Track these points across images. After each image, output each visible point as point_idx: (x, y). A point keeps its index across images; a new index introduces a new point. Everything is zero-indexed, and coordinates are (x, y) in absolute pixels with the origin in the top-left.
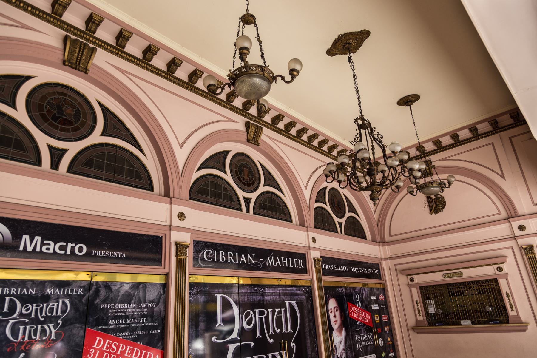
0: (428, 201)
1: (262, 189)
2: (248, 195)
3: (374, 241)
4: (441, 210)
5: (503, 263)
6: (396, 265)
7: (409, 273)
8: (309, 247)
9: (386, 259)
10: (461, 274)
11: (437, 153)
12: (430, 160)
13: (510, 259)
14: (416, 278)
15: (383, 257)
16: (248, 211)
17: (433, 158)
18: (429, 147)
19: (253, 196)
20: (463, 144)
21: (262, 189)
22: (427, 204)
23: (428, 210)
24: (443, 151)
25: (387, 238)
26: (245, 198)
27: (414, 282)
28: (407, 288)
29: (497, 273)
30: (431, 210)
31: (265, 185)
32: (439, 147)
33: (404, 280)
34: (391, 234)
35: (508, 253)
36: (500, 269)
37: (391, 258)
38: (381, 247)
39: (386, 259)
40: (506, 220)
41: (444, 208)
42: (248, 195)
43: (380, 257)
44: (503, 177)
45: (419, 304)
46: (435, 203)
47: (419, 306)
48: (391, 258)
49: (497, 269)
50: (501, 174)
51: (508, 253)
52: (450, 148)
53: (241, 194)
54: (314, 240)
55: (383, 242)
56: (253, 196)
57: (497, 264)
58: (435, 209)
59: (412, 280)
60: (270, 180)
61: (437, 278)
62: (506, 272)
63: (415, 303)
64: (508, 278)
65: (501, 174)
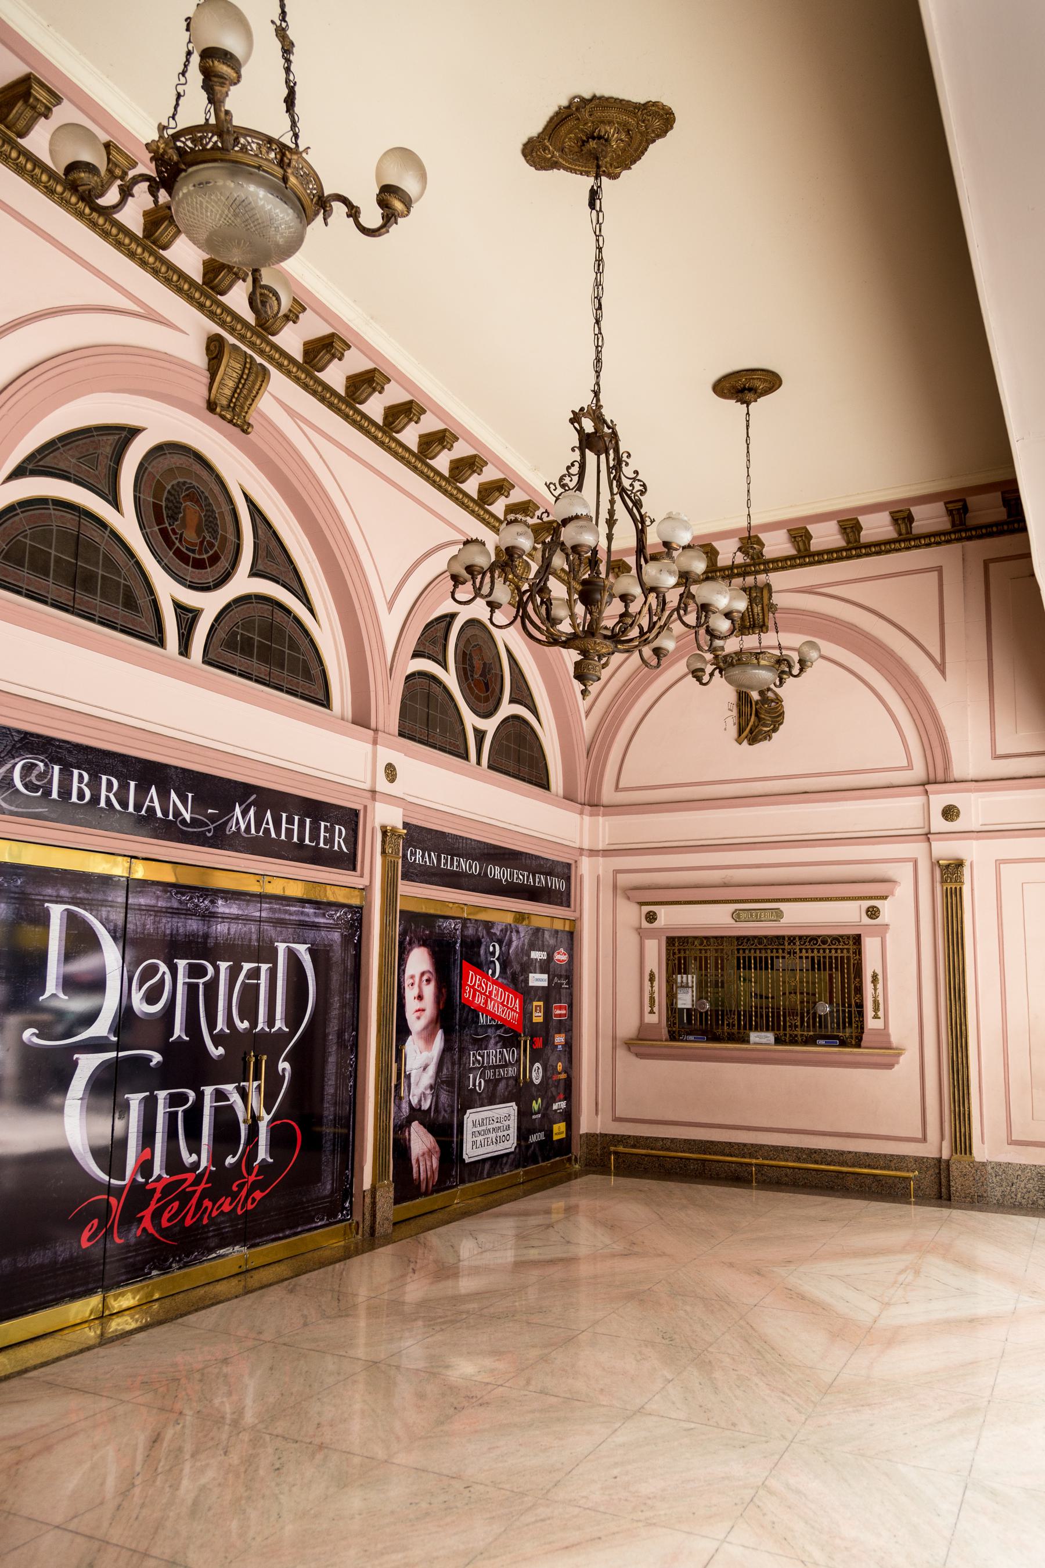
0: (739, 706)
1: (242, 583)
2: (191, 598)
3: (569, 797)
4: (768, 736)
5: (885, 898)
6: (617, 872)
7: (649, 898)
8: (373, 792)
9: (593, 853)
10: (779, 914)
11: (793, 567)
12: (768, 586)
13: (903, 891)
14: (662, 911)
15: (586, 846)
16: (185, 649)
17: (777, 580)
18: (777, 545)
19: (210, 604)
20: (867, 555)
21: (242, 583)
22: (735, 713)
23: (733, 730)
24: (811, 564)
25: (608, 794)
26: (179, 607)
27: (655, 925)
28: (634, 938)
29: (866, 920)
30: (740, 732)
31: (254, 573)
32: (804, 553)
33: (630, 914)
34: (621, 786)
35: (903, 874)
36: (873, 913)
37: (607, 853)
38: (587, 819)
39: (593, 853)
40: (921, 788)
41: (775, 730)
42: (191, 598)
43: (577, 845)
44: (942, 668)
45: (656, 984)
46: (757, 715)
47: (656, 989)
48: (607, 853)
49: (868, 911)
50: (938, 660)
51: (903, 874)
52: (830, 561)
53: (167, 589)
54: (391, 772)
55: (594, 804)
56: (210, 604)
57: (871, 898)
58: (751, 732)
59: (651, 917)
60: (274, 560)
61: (715, 919)
62: (886, 921)
63: (647, 977)
64: (888, 935)
65: (938, 659)
